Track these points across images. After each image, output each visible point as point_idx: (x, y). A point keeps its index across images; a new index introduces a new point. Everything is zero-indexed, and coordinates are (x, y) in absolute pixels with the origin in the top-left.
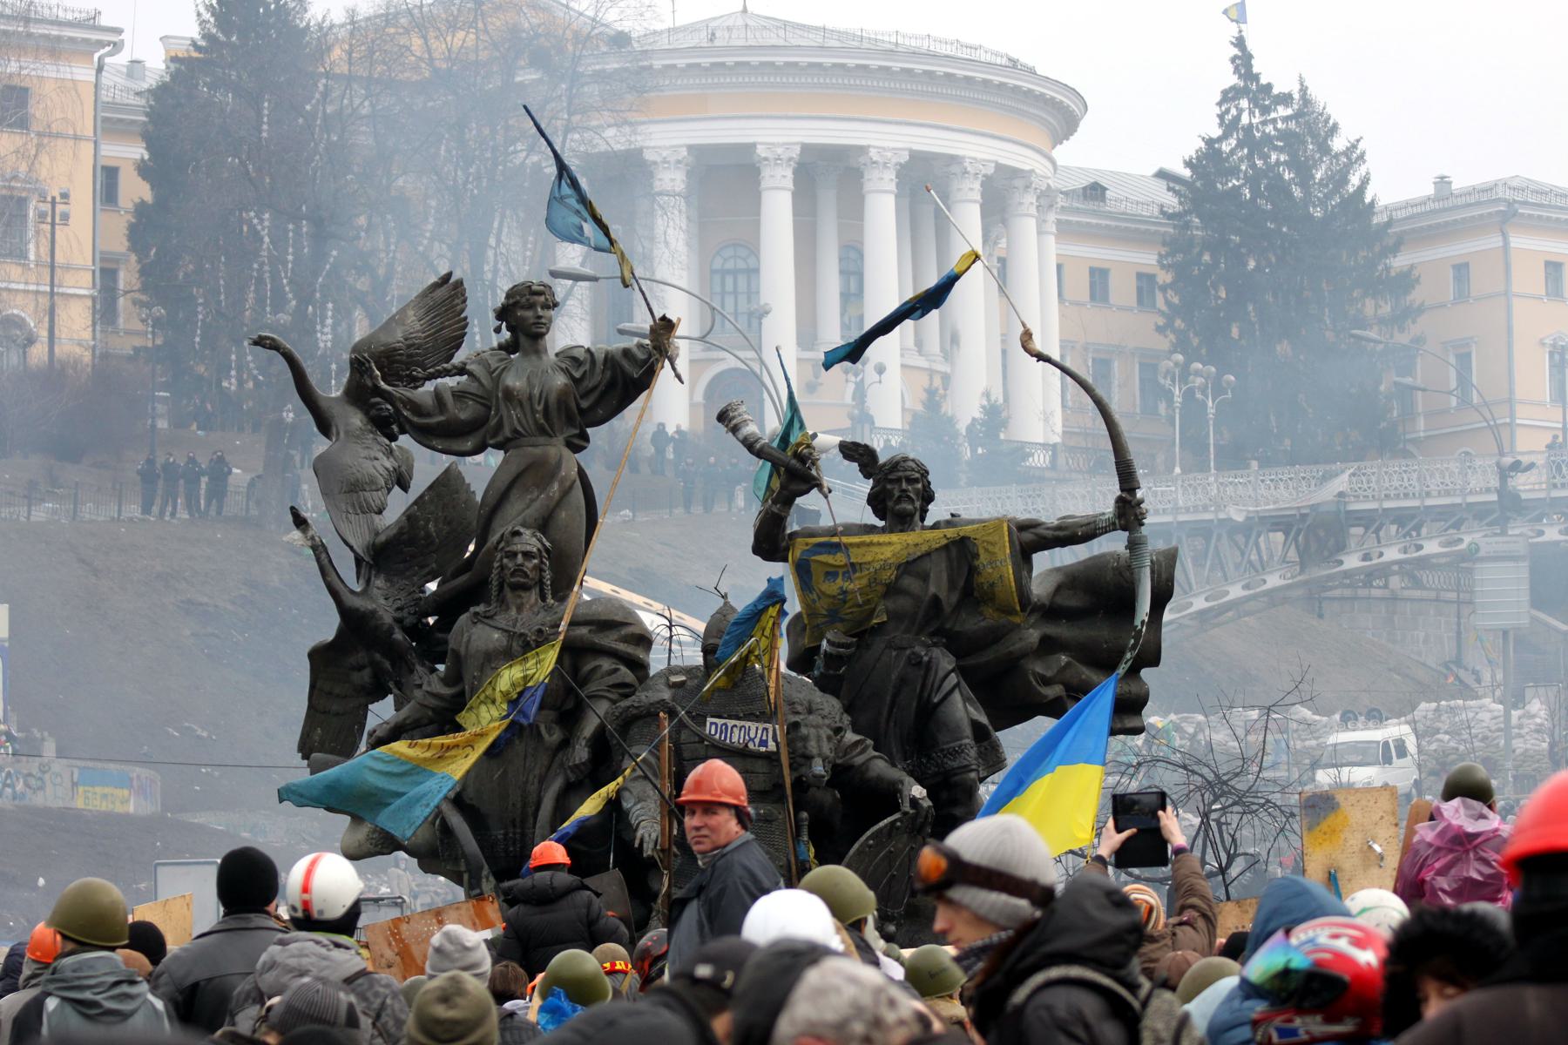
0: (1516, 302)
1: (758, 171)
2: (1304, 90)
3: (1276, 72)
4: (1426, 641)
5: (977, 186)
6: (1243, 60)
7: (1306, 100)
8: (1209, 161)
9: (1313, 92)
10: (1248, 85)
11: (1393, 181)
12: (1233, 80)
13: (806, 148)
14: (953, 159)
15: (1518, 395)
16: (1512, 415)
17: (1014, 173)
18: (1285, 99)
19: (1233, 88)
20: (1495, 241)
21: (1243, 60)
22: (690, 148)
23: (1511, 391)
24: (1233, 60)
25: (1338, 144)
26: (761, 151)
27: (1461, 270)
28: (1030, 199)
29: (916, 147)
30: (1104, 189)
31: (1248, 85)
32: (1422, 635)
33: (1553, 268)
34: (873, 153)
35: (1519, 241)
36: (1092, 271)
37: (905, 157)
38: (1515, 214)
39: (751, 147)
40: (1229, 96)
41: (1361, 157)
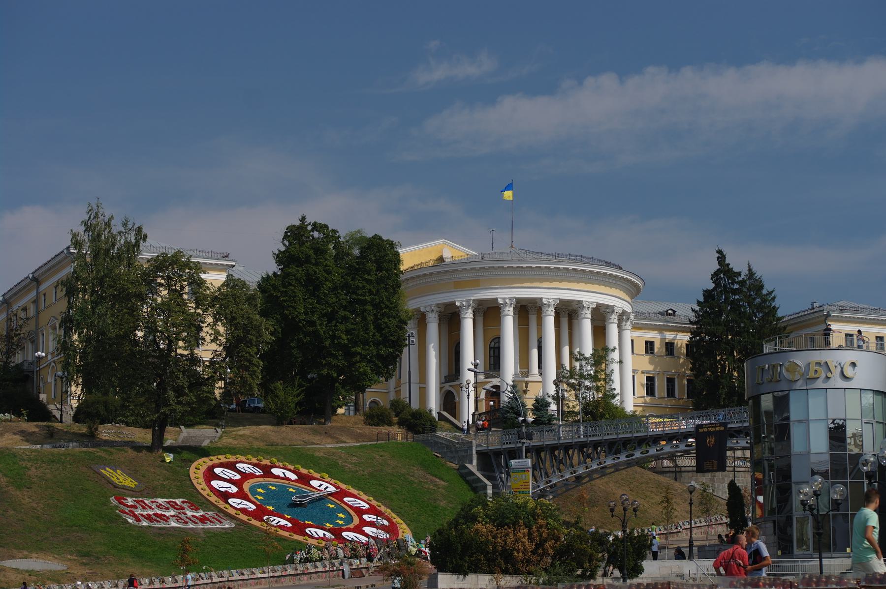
1: (500, 308)
2: (750, 270)
3: (737, 263)
5: (589, 312)
6: (721, 258)
7: (751, 273)
9: (754, 270)
13: (518, 300)
14: (580, 302)
17: (608, 307)
18: (739, 274)
19: (718, 270)
21: (721, 258)
24: (718, 258)
25: (764, 292)
26: (500, 301)
28: (614, 318)
30: (674, 312)
34: (545, 301)
39: (496, 299)
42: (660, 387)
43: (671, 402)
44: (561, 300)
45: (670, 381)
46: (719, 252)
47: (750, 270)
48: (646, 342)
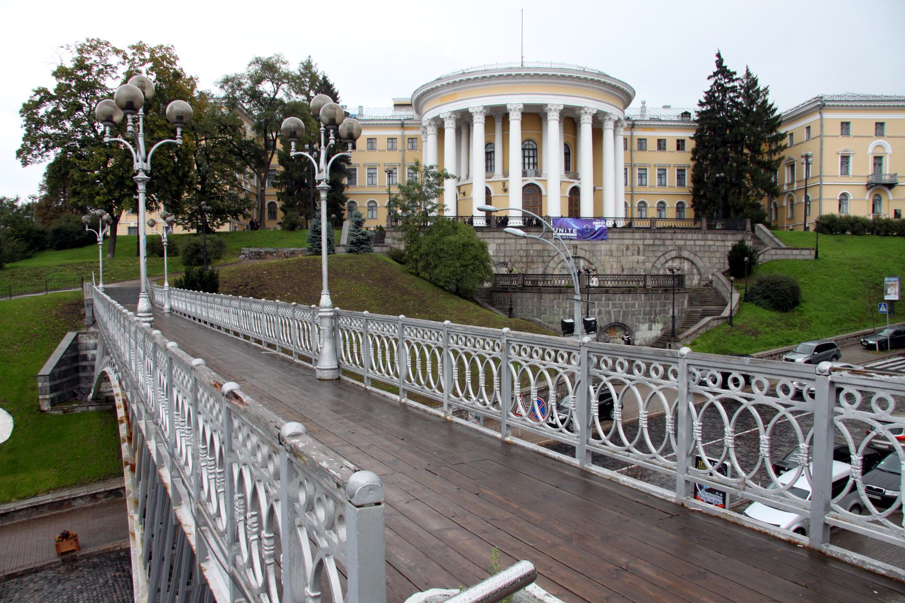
0: (825, 140)
2: (747, 70)
4: (600, 313)
6: (719, 63)
7: (748, 74)
8: (710, 97)
9: (751, 71)
10: (722, 70)
11: (782, 101)
12: (716, 69)
14: (547, 105)
15: (824, 173)
16: (821, 181)
17: (581, 108)
18: (735, 73)
20: (817, 116)
21: (719, 63)
22: (455, 112)
23: (821, 172)
26: (470, 111)
27: (808, 128)
29: (526, 102)
31: (722, 70)
32: (597, 311)
33: (845, 125)
34: (509, 107)
35: (827, 115)
36: (678, 141)
37: (521, 106)
38: (824, 105)
40: (715, 74)
41: (767, 93)
42: (671, 177)
43: (681, 190)
44: (525, 106)
45: (681, 172)
46: (718, 55)
47: (747, 70)
48: (659, 141)
